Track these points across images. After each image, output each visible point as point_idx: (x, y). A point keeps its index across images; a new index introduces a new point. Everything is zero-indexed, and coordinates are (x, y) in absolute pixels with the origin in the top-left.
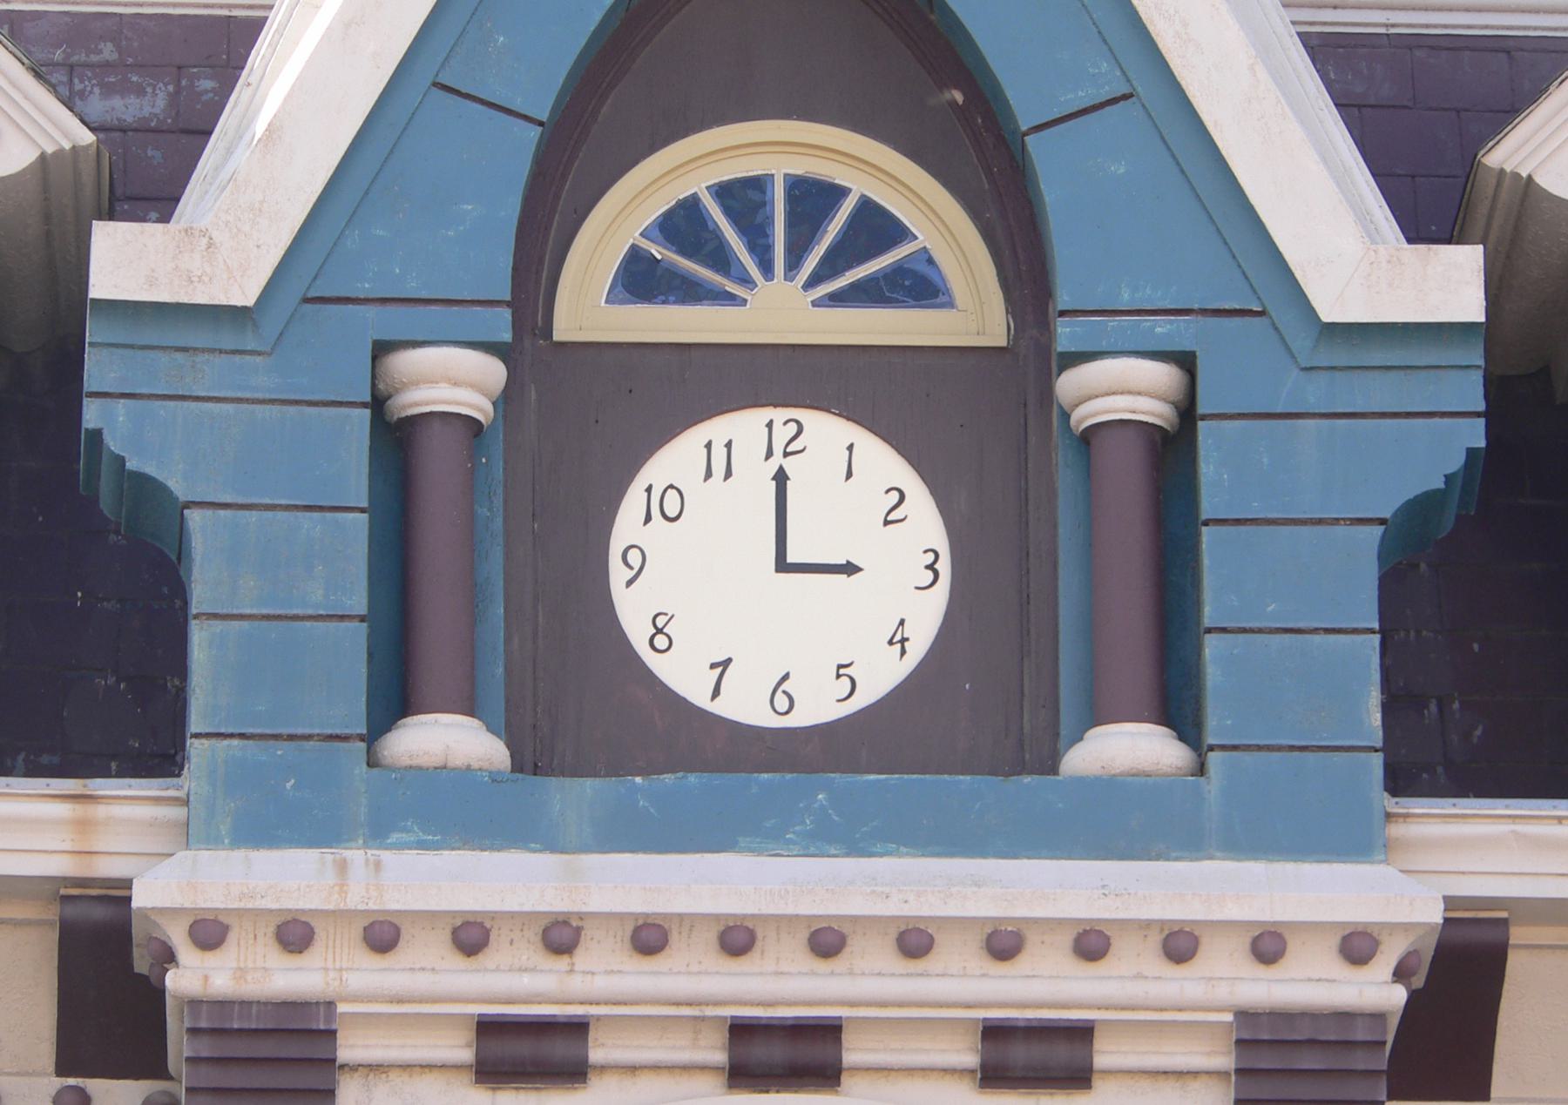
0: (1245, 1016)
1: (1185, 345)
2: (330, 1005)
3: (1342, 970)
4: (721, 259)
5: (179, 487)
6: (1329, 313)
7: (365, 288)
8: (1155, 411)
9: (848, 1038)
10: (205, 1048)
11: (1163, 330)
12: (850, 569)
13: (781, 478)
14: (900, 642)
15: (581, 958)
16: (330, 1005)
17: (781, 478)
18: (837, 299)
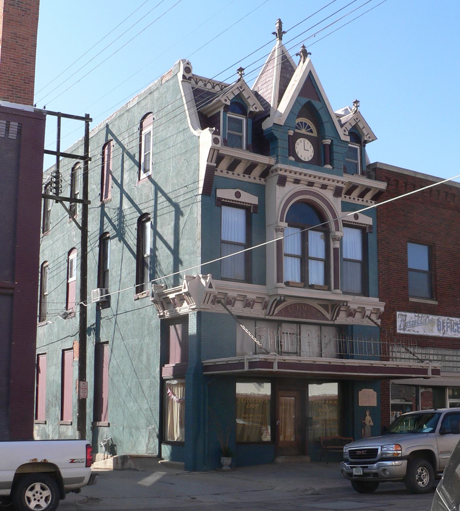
0: (336, 186)
1: (332, 139)
2: (287, 176)
3: (337, 183)
4: (300, 127)
5: (277, 137)
6: (342, 139)
7: (288, 125)
8: (329, 143)
9: (315, 184)
10: (280, 178)
11: (332, 138)
12: (308, 150)
13: (304, 143)
14: (311, 156)
15: (301, 176)
16: (287, 176)
17: (304, 143)
18: (307, 131)
